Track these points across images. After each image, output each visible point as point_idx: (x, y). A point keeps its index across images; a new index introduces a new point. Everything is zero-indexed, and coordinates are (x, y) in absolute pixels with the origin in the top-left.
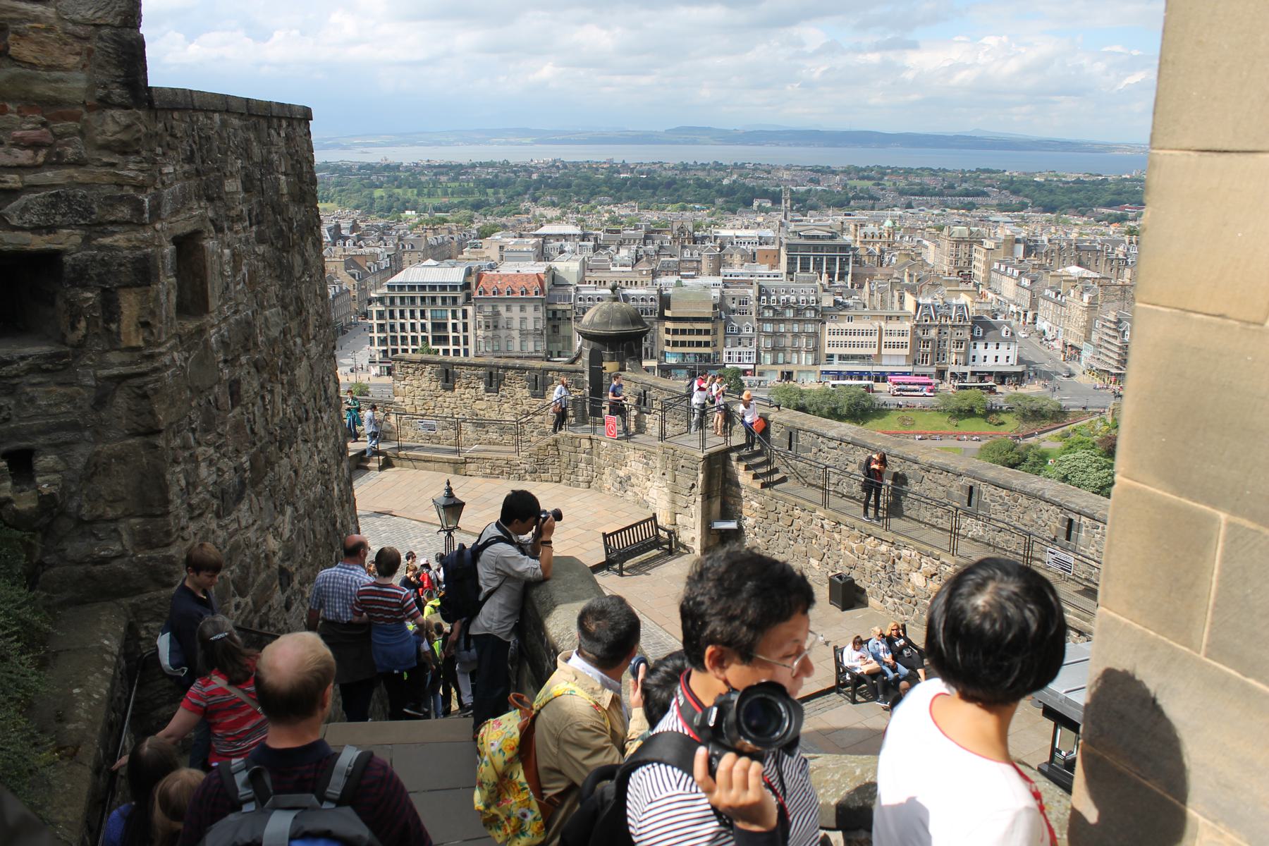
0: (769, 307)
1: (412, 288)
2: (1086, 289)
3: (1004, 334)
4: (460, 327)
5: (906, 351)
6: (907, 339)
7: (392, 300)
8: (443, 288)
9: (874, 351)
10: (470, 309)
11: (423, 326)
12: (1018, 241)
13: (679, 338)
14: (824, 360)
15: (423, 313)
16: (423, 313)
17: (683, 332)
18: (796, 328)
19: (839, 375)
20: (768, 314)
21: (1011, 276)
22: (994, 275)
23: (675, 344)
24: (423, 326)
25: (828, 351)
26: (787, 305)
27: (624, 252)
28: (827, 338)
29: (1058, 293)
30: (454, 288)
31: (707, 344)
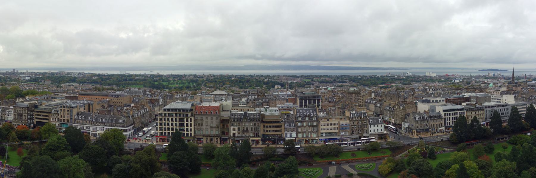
0: (300, 117)
1: (172, 110)
7: (165, 114)
8: (183, 110)
10: (193, 118)
13: (268, 129)
14: (320, 135)
15: (176, 120)
16: (176, 120)
17: (270, 127)
19: (325, 141)
20: (300, 119)
24: (176, 124)
25: (322, 132)
26: (306, 116)
30: (187, 110)
31: (278, 131)
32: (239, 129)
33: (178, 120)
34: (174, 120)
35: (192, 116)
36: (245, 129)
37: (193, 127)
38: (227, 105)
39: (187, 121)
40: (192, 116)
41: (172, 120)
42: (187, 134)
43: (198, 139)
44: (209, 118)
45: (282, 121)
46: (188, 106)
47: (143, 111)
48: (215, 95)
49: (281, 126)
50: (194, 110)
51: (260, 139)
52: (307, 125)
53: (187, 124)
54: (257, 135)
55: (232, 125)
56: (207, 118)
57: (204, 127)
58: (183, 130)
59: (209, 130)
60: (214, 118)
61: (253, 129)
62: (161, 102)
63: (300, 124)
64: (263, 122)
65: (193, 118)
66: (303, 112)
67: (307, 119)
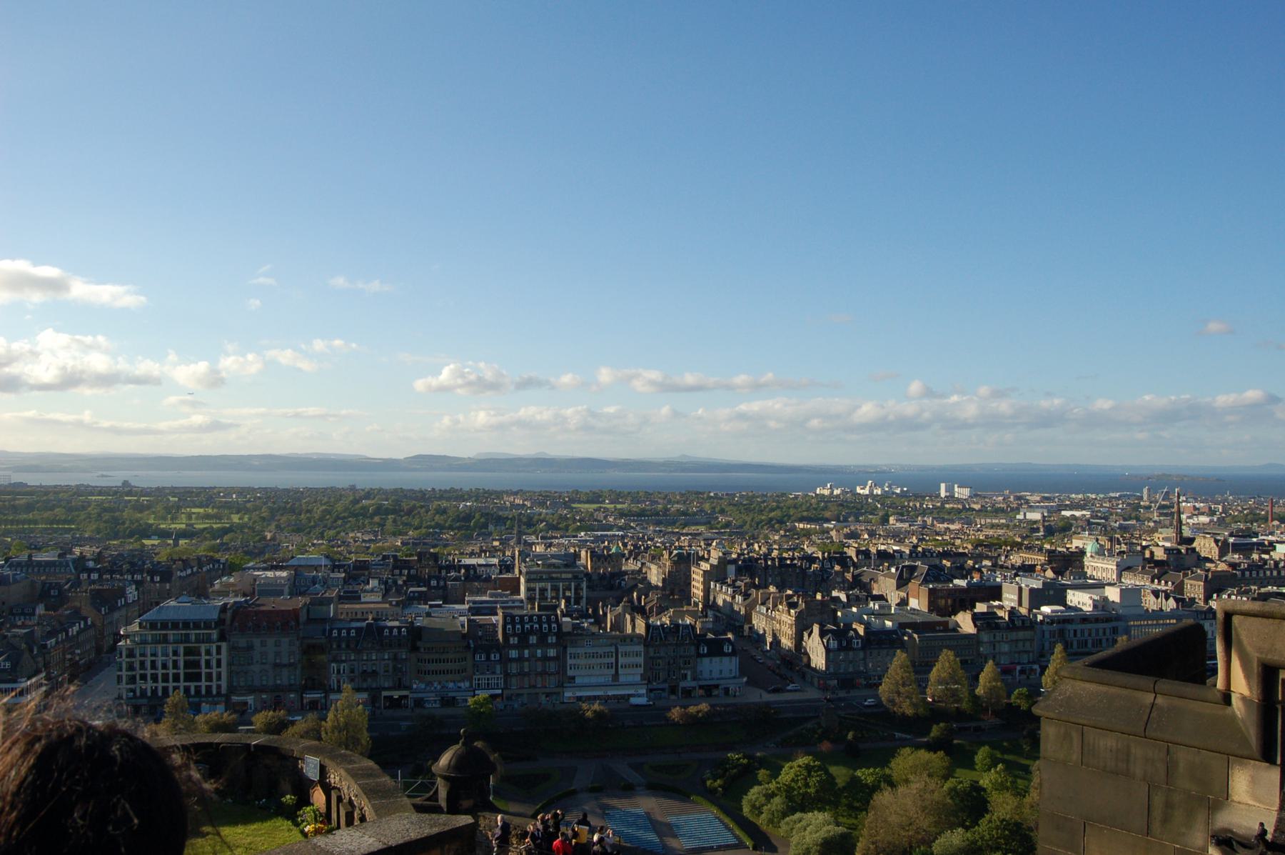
0: (514, 635)
4: (214, 663)
5: (641, 670)
6: (641, 660)
16: (175, 653)
25: (570, 673)
26: (531, 632)
27: (373, 583)
28: (569, 662)
30: (207, 625)
32: (352, 671)
33: (181, 651)
35: (222, 637)
40: (222, 637)
44: (271, 642)
47: (76, 628)
50: (228, 622)
52: (533, 655)
54: (399, 686)
55: (335, 660)
56: (263, 644)
57: (256, 668)
58: (197, 677)
60: (285, 640)
62: (132, 593)
63: (514, 654)
64: (415, 649)
65: (224, 645)
67: (533, 639)
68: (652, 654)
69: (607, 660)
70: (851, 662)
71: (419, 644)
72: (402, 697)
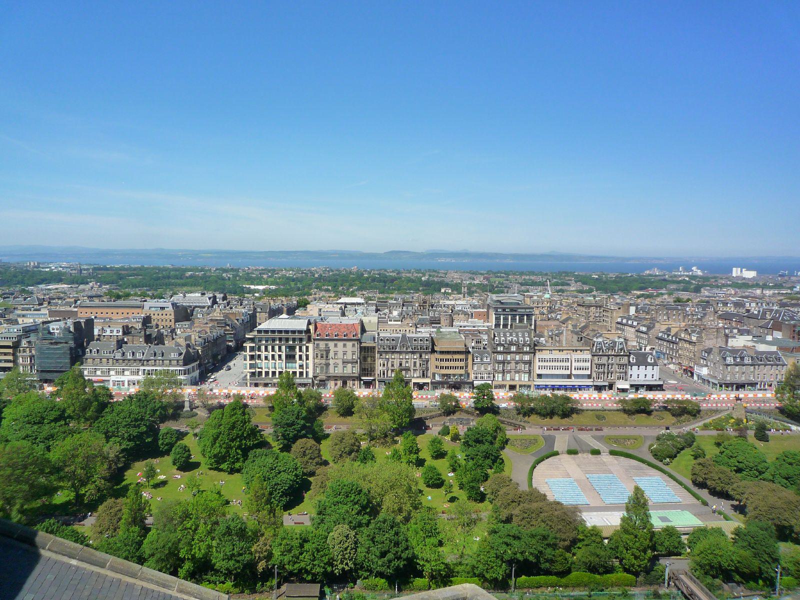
0: (500, 345)
1: (273, 332)
2: (694, 332)
3: (649, 360)
4: (304, 357)
6: (589, 364)
9: (568, 372)
10: (311, 346)
11: (280, 356)
12: (631, 305)
14: (535, 376)
15: (280, 349)
18: (517, 357)
20: (500, 349)
21: (632, 326)
22: (619, 326)
23: (442, 368)
24: (280, 356)
26: (511, 344)
27: (395, 313)
28: (537, 364)
29: (668, 335)
30: (300, 332)
32: (393, 365)
33: (283, 348)
34: (277, 348)
36: (403, 365)
37: (310, 362)
38: (370, 322)
39: (300, 350)
40: (309, 340)
41: (273, 350)
42: (301, 374)
43: (320, 381)
44: (340, 344)
45: (469, 352)
46: (301, 325)
48: (346, 304)
49: (467, 359)
50: (312, 331)
51: (428, 380)
53: (300, 357)
54: (424, 375)
59: (341, 365)
61: (418, 365)
63: (500, 357)
64: (433, 351)
65: (311, 346)
66: (505, 336)
68: (596, 362)
69: (564, 364)
70: (743, 373)
71: (436, 348)
72: (425, 384)
